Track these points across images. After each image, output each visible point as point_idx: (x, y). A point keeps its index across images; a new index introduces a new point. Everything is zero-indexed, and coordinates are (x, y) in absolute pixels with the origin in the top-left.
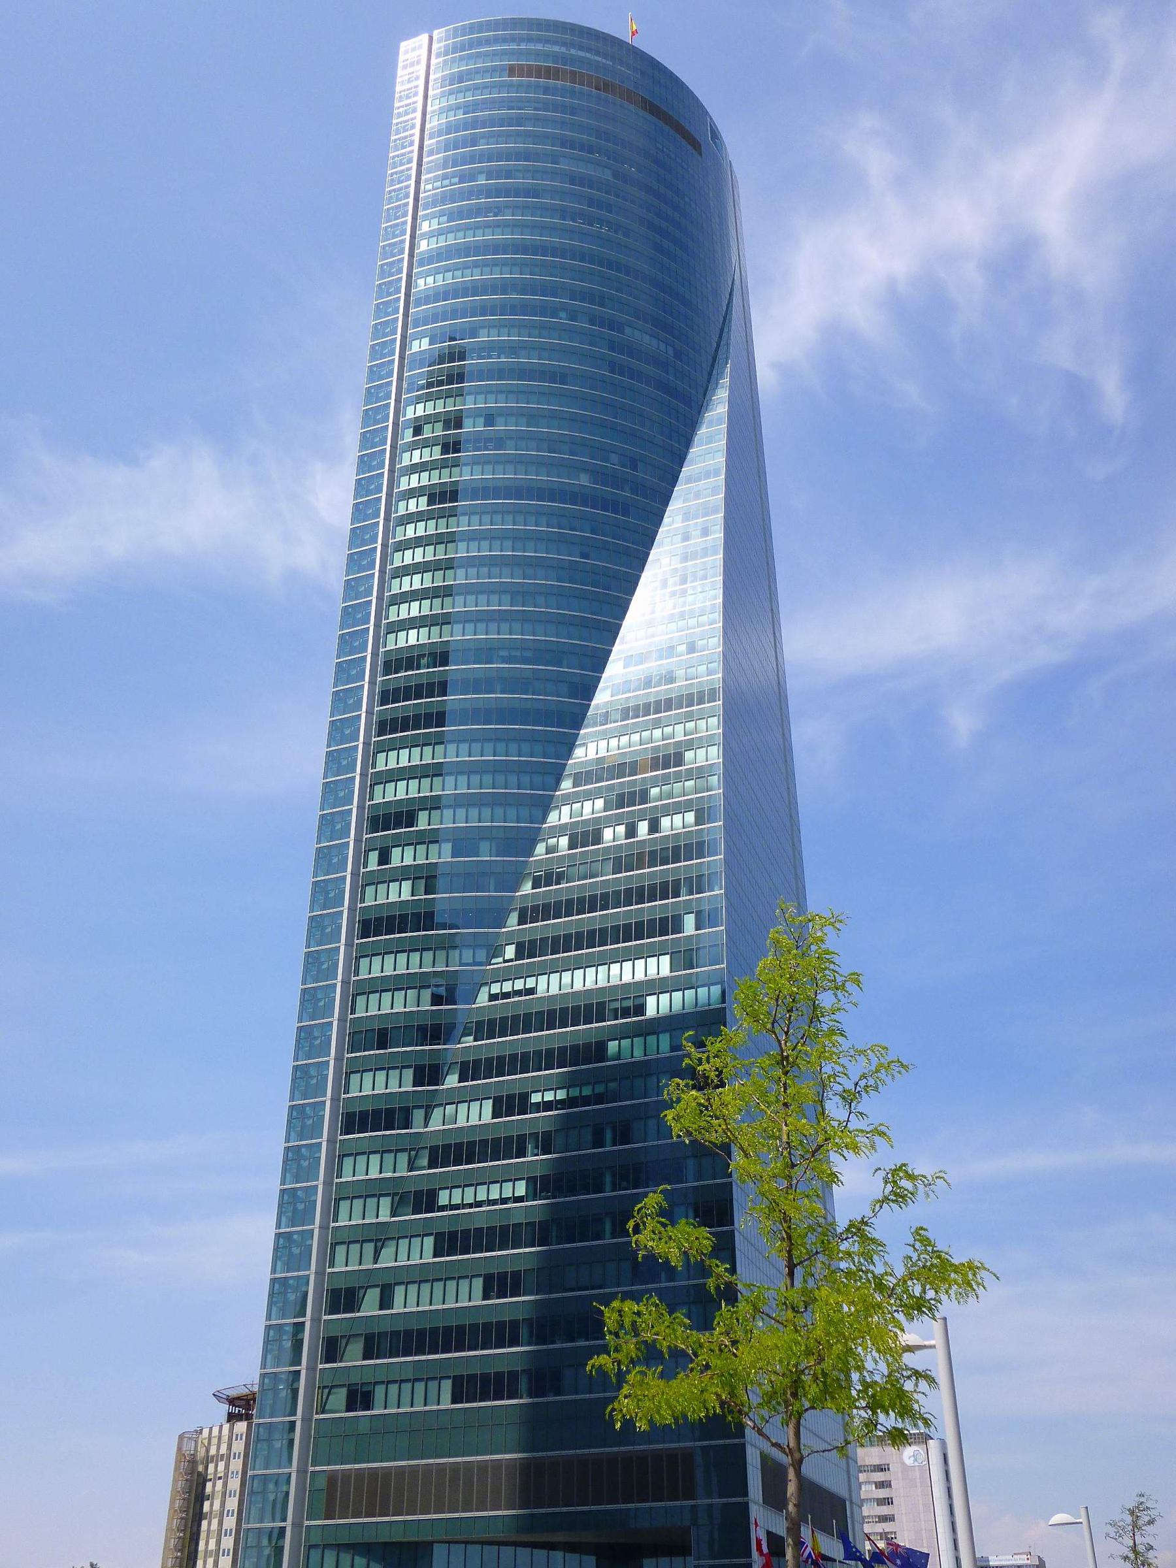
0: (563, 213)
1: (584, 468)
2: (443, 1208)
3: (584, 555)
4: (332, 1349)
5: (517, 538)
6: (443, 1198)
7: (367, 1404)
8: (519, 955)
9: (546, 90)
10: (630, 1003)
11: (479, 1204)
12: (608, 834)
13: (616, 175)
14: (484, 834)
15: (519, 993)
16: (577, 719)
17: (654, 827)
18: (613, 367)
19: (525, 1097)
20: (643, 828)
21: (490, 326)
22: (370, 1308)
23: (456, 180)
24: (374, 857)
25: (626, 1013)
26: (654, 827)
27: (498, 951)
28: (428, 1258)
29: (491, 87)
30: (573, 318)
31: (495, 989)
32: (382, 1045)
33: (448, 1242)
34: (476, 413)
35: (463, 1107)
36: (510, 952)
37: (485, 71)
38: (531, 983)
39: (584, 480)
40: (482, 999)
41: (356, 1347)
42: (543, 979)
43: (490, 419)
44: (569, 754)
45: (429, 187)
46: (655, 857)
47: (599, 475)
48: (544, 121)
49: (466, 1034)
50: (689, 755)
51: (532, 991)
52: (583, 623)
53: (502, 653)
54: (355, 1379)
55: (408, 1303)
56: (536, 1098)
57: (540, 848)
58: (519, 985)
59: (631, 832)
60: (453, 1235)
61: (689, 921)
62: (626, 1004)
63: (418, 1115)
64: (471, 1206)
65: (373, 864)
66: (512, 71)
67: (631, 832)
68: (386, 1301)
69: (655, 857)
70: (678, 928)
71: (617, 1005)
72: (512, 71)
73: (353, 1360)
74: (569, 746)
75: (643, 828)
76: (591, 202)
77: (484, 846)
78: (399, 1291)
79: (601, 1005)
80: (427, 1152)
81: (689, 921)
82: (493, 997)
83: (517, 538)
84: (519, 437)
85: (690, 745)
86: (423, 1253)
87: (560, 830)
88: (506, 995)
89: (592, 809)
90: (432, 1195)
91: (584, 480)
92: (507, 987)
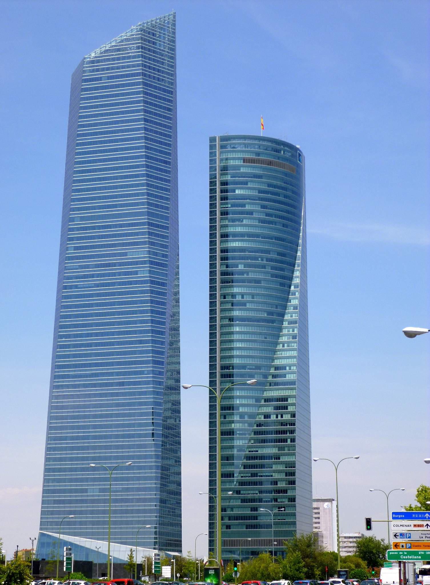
1: (264, 311)
3: (266, 338)
4: (222, 519)
6: (242, 492)
14: (246, 413)
17: (282, 417)
18: (273, 276)
19: (257, 474)
20: (279, 416)
22: (229, 512)
26: (282, 417)
27: (250, 440)
32: (227, 460)
34: (239, 294)
36: (252, 442)
41: (227, 518)
43: (243, 297)
46: (282, 424)
47: (270, 313)
51: (257, 451)
52: (266, 358)
53: (248, 367)
55: (236, 512)
56: (259, 474)
58: (255, 449)
59: (277, 417)
61: (289, 440)
67: (277, 417)
69: (282, 424)
70: (287, 442)
73: (227, 521)
75: (279, 416)
77: (246, 417)
81: (289, 440)
85: (290, 397)
86: (239, 503)
88: (252, 451)
90: (240, 491)
92: (252, 450)
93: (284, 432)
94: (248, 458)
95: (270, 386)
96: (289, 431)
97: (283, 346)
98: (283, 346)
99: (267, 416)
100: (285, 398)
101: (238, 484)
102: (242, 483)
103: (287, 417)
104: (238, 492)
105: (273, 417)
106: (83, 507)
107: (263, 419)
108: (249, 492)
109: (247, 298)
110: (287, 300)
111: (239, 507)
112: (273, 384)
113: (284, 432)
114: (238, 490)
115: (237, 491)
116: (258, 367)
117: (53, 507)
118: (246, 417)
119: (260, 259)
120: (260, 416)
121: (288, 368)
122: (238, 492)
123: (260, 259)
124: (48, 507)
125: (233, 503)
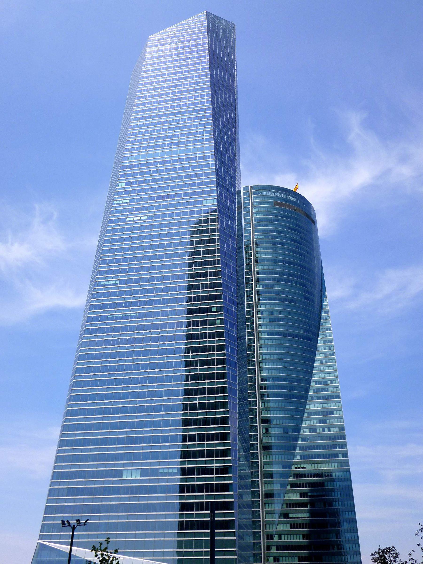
0: (291, 250)
2: (290, 518)
3: (304, 353)
5: (290, 348)
6: (290, 515)
7: (278, 561)
8: (301, 458)
9: (284, 211)
10: (329, 474)
11: (299, 518)
12: (318, 430)
13: (301, 238)
15: (302, 468)
16: (306, 398)
17: (329, 430)
20: (326, 430)
21: (278, 285)
23: (263, 237)
24: (264, 430)
25: (328, 476)
26: (329, 430)
28: (289, 529)
29: (270, 208)
30: (296, 283)
31: (296, 466)
33: (293, 526)
35: (292, 494)
36: (299, 457)
37: (268, 203)
38: (305, 466)
39: (302, 332)
40: (293, 469)
42: (307, 465)
44: (305, 408)
45: (256, 237)
46: (330, 438)
48: (284, 221)
49: (290, 476)
50: (335, 412)
51: (305, 468)
54: (275, 555)
55: (285, 539)
57: (302, 431)
58: (302, 466)
59: (324, 431)
60: (294, 524)
61: (340, 455)
62: (328, 474)
63: (282, 495)
64: (297, 518)
65: (264, 432)
66: (274, 203)
67: (324, 431)
68: (280, 538)
69: (330, 438)
70: (338, 457)
71: (326, 474)
72: (274, 203)
73: (274, 551)
74: (305, 405)
75: (326, 430)
76: (297, 247)
78: (283, 536)
79: (322, 473)
80: (285, 504)
81: (340, 455)
82: (296, 468)
83: (290, 348)
84: (288, 319)
86: (287, 528)
87: (306, 427)
88: (299, 468)
89: (313, 423)
91: (302, 332)
92: (299, 466)
93: (334, 446)
94: (296, 476)
95: (312, 400)
96: (339, 445)
97: (322, 362)
98: (322, 362)
99: (313, 430)
100: (330, 412)
101: (285, 507)
102: (290, 505)
103: (335, 431)
104: (286, 515)
105: (319, 431)
106: (114, 500)
107: (308, 433)
108: (300, 515)
109: (283, 316)
110: (319, 324)
111: (287, 533)
112: (316, 398)
113: (334, 446)
114: (286, 512)
115: (285, 514)
116: (299, 380)
117: (66, 501)
118: (290, 430)
119: (293, 282)
120: (305, 430)
121: (329, 382)
122: (286, 515)
123: (293, 282)
124: (57, 501)
125: (280, 528)
